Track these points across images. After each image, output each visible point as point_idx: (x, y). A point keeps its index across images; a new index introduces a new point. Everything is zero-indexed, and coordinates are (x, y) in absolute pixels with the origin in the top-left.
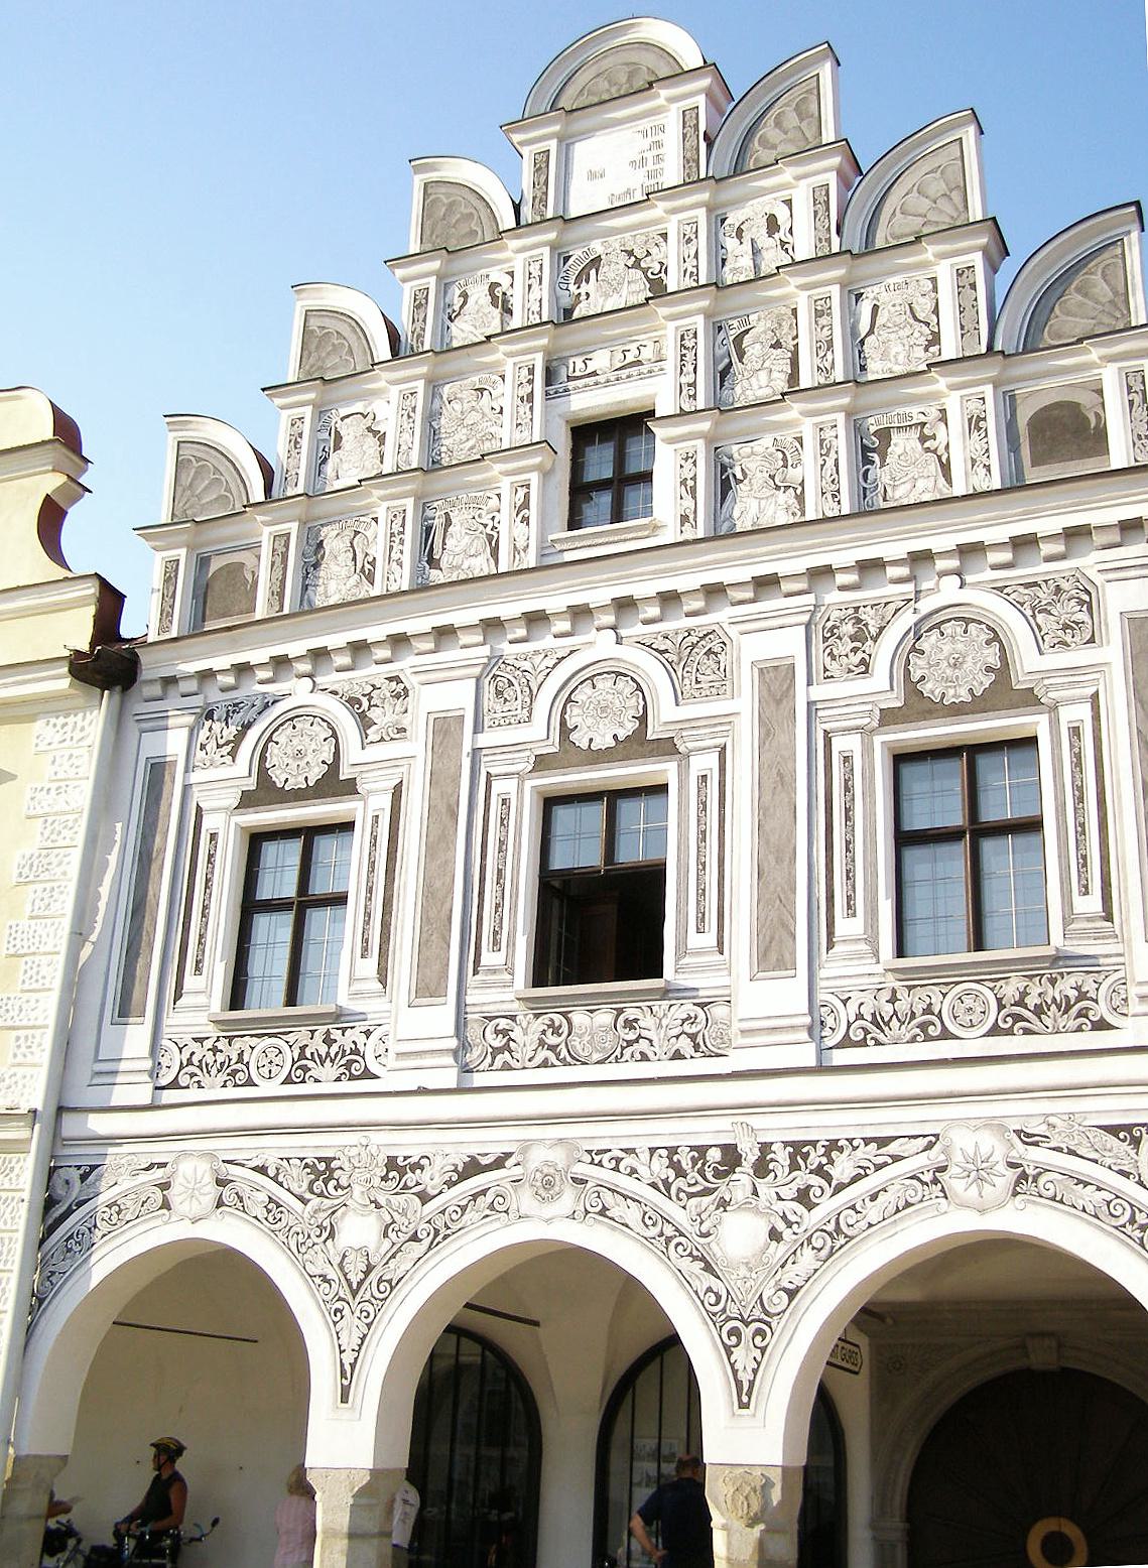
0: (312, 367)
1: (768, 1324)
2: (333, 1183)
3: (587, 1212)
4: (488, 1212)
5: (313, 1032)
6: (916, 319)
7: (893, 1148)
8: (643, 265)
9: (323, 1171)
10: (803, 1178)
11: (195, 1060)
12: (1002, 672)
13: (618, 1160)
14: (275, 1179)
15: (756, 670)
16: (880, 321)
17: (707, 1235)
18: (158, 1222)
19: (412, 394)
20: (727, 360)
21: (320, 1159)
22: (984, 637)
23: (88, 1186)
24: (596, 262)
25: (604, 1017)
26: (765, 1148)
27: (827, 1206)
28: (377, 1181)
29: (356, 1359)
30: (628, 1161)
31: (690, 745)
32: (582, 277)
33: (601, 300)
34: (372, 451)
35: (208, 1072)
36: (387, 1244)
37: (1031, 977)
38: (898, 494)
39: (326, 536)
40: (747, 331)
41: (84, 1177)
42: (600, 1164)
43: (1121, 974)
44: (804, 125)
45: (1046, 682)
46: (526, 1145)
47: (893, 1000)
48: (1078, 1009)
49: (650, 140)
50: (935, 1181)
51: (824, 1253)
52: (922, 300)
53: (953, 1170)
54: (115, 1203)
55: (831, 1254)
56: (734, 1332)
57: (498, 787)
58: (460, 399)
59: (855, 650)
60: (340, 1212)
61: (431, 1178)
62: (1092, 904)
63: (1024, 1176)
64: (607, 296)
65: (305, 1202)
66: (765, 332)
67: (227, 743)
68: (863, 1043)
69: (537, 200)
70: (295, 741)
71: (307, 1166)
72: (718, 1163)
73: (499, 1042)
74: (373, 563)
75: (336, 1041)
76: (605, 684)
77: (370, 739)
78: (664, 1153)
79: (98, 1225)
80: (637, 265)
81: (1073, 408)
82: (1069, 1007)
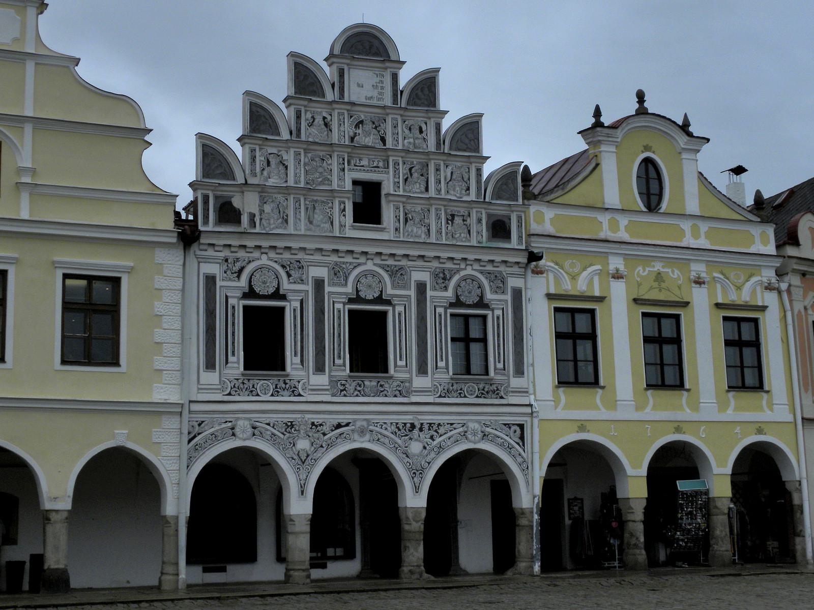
0: (255, 127)
1: (423, 471)
2: (293, 429)
3: (374, 440)
4: (344, 439)
5: (279, 380)
6: (464, 180)
7: (454, 426)
8: (378, 129)
9: (290, 425)
10: (432, 432)
11: (236, 386)
12: (481, 297)
13: (382, 426)
14: (273, 427)
15: (416, 283)
16: (454, 177)
17: (406, 447)
18: (231, 440)
19: (299, 154)
20: (406, 176)
21: (289, 422)
22: (477, 286)
23: (202, 428)
24: (362, 122)
25: (374, 383)
26: (422, 424)
27: (438, 440)
28: (308, 429)
29: (305, 483)
30: (384, 426)
31: (395, 302)
32: (357, 126)
33: (364, 138)
34: (283, 171)
35: (242, 391)
36: (313, 448)
37: (486, 383)
38: (456, 236)
39: (267, 200)
40: (413, 167)
41: (199, 425)
42: (377, 426)
43: (506, 385)
44: (430, 95)
45: (492, 302)
46: (355, 421)
47: (452, 386)
48: (496, 393)
49: (378, 80)
50: (464, 435)
51: (437, 453)
52: (466, 174)
53: (469, 433)
54: (213, 434)
55: (439, 453)
56: (414, 473)
57: (337, 306)
58: (316, 162)
59: (443, 283)
60: (296, 439)
61: (325, 429)
62: (500, 366)
63: (485, 435)
64: (366, 137)
65: (284, 435)
66: (419, 169)
67: (236, 273)
68: (445, 397)
69: (341, 90)
70: (263, 277)
71: (284, 423)
72: (410, 428)
73: (342, 388)
74: (287, 216)
75: (287, 383)
76: (370, 278)
77: (291, 281)
78: (395, 424)
79: (207, 441)
80: (376, 128)
81: (504, 222)
82: (494, 392)
